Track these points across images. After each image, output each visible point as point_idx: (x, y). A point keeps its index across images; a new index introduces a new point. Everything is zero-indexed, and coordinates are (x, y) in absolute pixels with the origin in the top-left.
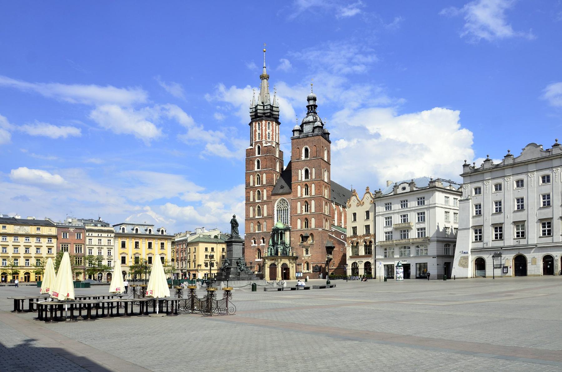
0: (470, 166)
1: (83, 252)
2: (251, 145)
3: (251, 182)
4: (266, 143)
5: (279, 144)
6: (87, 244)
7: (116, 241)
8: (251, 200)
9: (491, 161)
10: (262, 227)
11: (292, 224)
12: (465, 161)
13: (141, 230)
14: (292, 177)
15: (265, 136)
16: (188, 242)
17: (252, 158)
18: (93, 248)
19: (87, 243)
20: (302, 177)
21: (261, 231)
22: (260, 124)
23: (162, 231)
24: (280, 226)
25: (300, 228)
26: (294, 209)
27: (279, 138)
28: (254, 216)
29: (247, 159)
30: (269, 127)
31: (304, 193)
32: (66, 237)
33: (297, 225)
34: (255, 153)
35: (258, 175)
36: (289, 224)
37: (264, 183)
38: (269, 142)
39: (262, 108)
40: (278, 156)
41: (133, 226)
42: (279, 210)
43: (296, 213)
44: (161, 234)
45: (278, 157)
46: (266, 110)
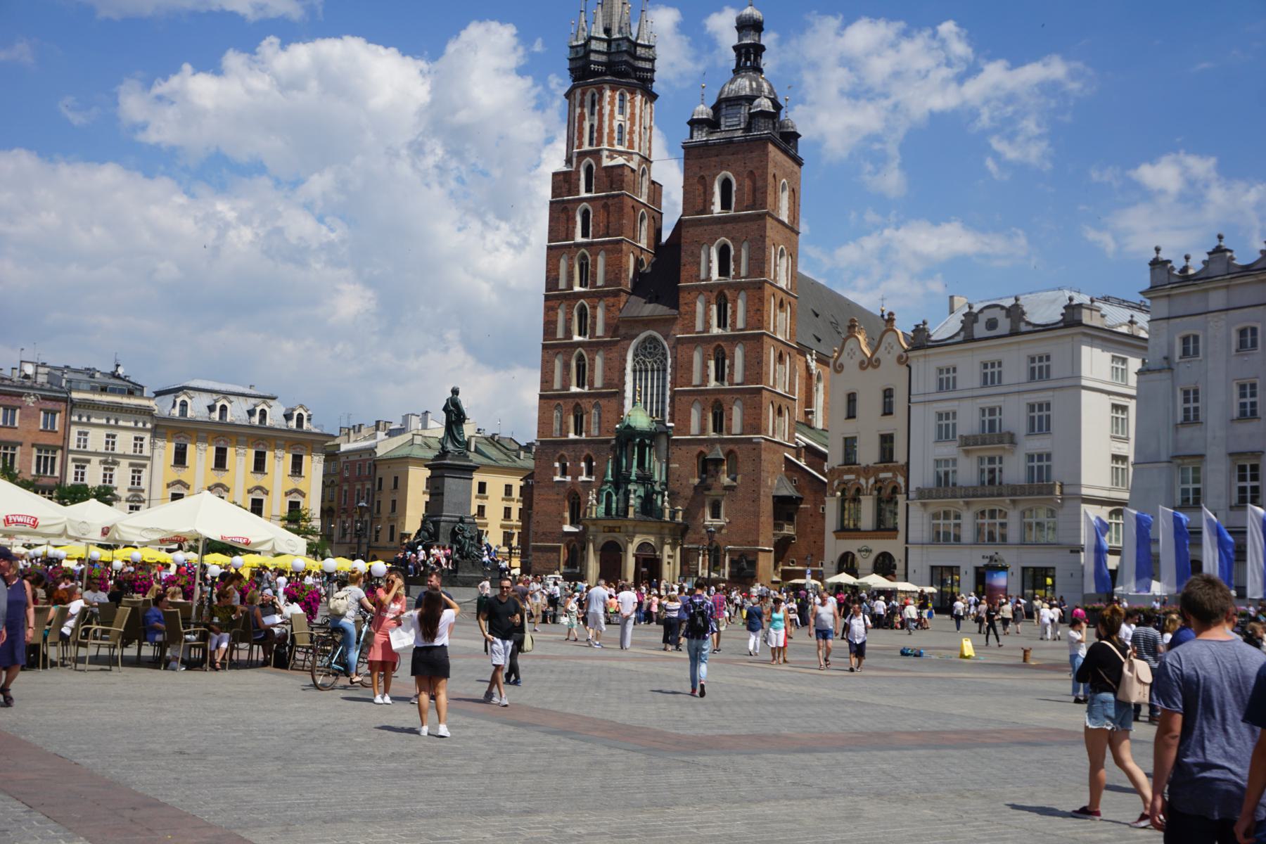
0: (1169, 265)
1: (57, 474)
2: (569, 161)
3: (560, 277)
4: (612, 158)
5: (651, 162)
6: (70, 448)
7: (160, 443)
9: (1229, 254)
10: (587, 422)
11: (676, 420)
12: (1158, 250)
13: (237, 412)
14: (682, 268)
15: (608, 133)
16: (378, 455)
17: (569, 200)
18: (88, 461)
19: (73, 445)
20: (709, 269)
21: (584, 434)
22: (597, 96)
23: (298, 418)
24: (640, 419)
25: (697, 433)
26: (683, 369)
27: (650, 142)
29: (554, 205)
31: (714, 321)
32: (13, 422)
33: (690, 421)
34: (578, 186)
35: (584, 257)
36: (667, 417)
37: (600, 282)
38: (621, 153)
40: (646, 197)
41: (215, 396)
42: (641, 371)
43: (690, 384)
44: (295, 427)
45: (645, 202)
46: (614, 53)
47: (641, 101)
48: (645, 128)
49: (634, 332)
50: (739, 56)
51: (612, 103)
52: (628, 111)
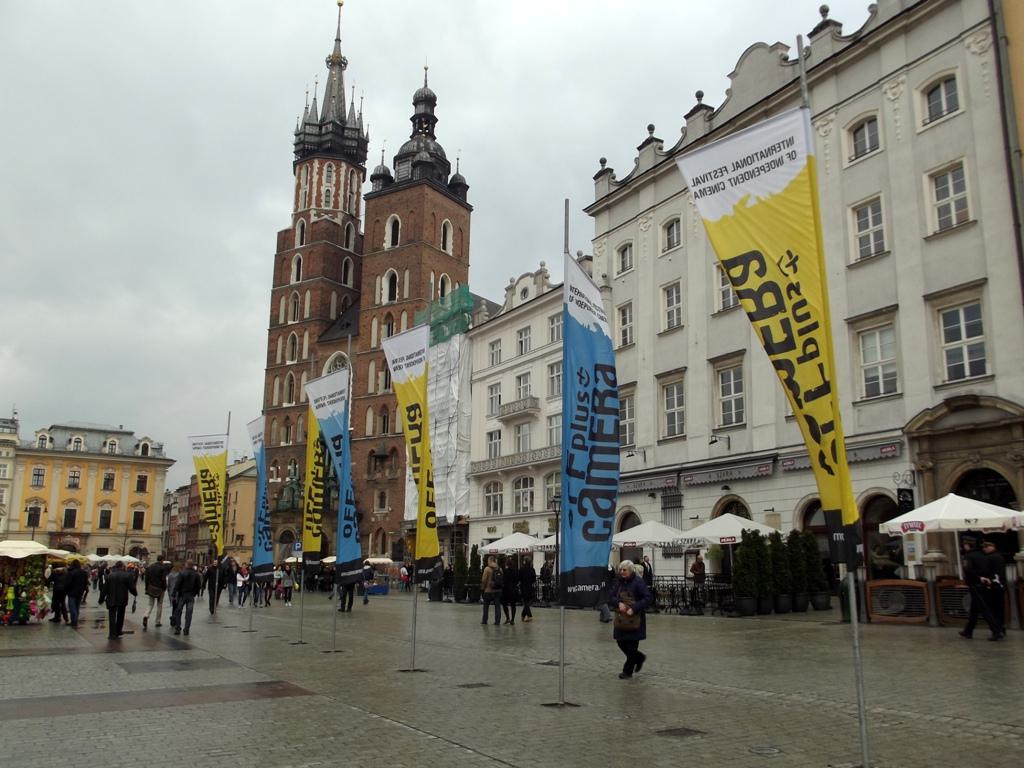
8: (279, 361)
25: (371, 434)
28: (280, 403)
30: (329, 177)
37: (307, 316)
39: (315, 130)
47: (347, 172)
48: (351, 192)
49: (325, 354)
50: (414, 125)
51: (320, 173)
52: (334, 178)
